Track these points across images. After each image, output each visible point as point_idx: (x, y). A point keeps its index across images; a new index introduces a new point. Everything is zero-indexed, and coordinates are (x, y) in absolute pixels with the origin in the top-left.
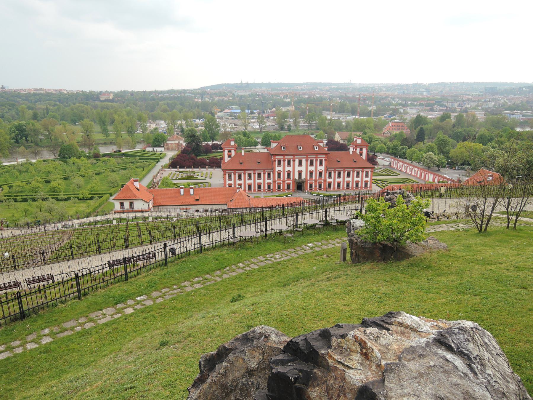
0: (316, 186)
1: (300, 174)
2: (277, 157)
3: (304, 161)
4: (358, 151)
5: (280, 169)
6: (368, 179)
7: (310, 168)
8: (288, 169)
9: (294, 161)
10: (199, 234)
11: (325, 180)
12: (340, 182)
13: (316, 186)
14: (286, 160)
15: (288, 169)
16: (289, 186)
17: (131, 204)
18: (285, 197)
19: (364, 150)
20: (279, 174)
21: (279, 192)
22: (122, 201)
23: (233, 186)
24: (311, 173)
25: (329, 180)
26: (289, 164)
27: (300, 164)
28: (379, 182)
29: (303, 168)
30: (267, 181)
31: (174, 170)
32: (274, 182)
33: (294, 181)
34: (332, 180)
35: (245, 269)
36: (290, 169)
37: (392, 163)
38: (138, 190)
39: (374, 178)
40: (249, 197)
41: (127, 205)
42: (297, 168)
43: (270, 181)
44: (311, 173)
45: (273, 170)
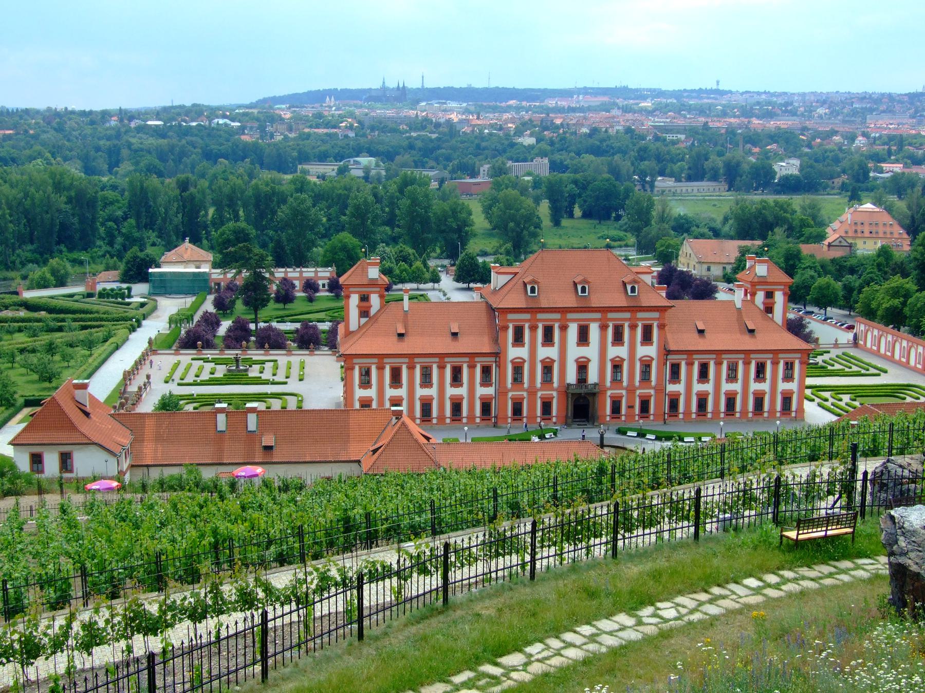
0: (631, 407)
1: (582, 367)
2: (510, 316)
3: (594, 331)
4: (760, 297)
5: (522, 352)
6: (793, 386)
7: (614, 352)
8: (544, 352)
9: (564, 328)
10: (781, 461)
11: (660, 390)
12: (707, 394)
13: (631, 407)
14: (540, 326)
15: (544, 352)
16: (547, 407)
17: (66, 461)
18: (536, 439)
20: (518, 369)
21: (517, 424)
22: (36, 450)
23: (374, 405)
24: (617, 367)
25: (671, 388)
26: (548, 338)
27: (583, 338)
28: (826, 395)
29: (591, 352)
30: (481, 391)
31: (186, 357)
32: (502, 392)
33: (566, 390)
34: (680, 388)
35: (761, 584)
36: (552, 353)
38: (87, 414)
39: (809, 381)
40: (428, 439)
41: (51, 463)
42: (574, 352)
43: (490, 391)
44: (617, 367)
45: (498, 355)
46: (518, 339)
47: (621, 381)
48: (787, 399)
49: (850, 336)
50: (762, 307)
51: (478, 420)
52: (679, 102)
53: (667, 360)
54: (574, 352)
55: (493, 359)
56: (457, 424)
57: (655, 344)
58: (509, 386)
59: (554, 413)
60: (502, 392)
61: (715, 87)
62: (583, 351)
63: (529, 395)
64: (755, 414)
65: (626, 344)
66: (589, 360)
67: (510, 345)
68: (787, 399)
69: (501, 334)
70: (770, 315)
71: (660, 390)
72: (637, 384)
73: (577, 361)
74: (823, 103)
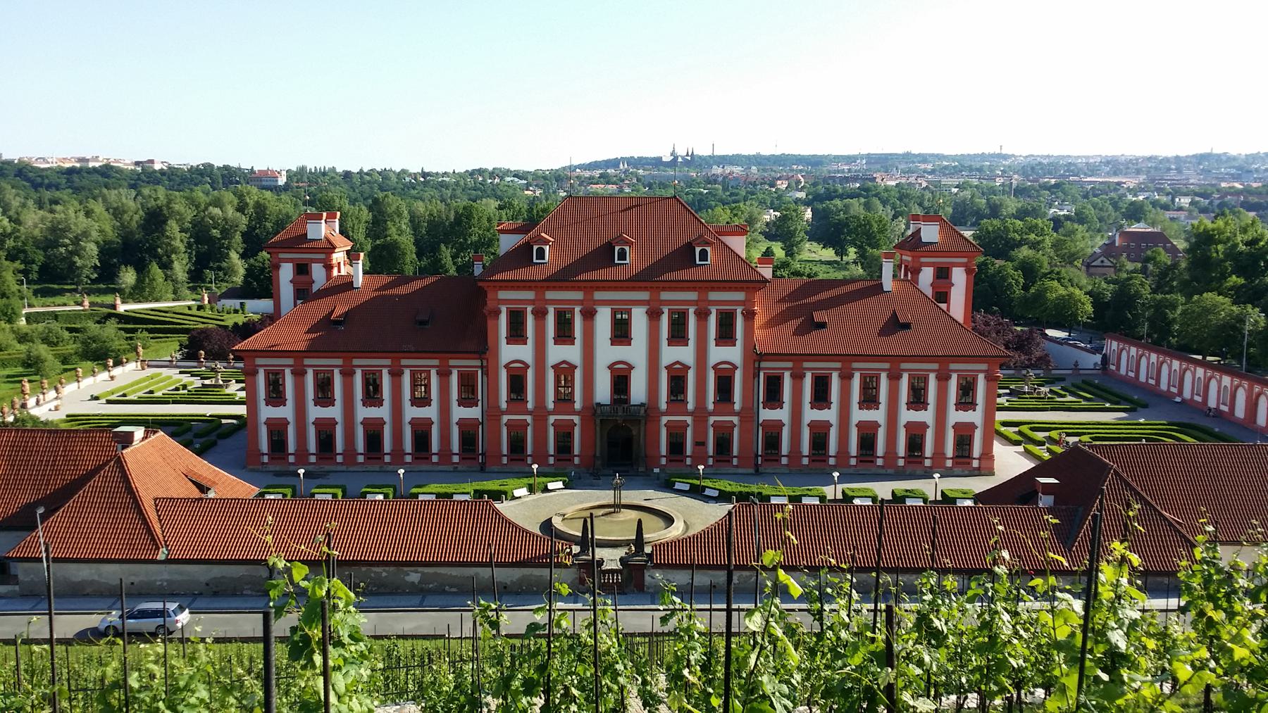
1: (621, 380)
5: (524, 352)
6: (975, 417)
7: (670, 354)
8: (556, 353)
9: (589, 315)
11: (749, 414)
14: (551, 310)
15: (556, 353)
19: (959, 277)
25: (766, 414)
26: (564, 335)
27: (621, 334)
28: (1040, 436)
30: (459, 413)
32: (492, 413)
33: (592, 411)
34: (782, 414)
36: (572, 353)
37: (1113, 359)
43: (474, 413)
46: (517, 335)
47: (685, 402)
48: (964, 436)
49: (1098, 358)
50: (929, 292)
51: (456, 459)
52: (963, 165)
53: (759, 369)
54: (607, 353)
55: (478, 363)
56: (517, 467)
57: (739, 343)
58: (504, 406)
59: (576, 451)
60: (492, 413)
61: (998, 151)
62: (621, 353)
63: (534, 420)
64: (368, 458)
65: (692, 342)
66: (631, 367)
67: (503, 341)
68: (964, 436)
69: (490, 323)
70: (943, 306)
71: (749, 414)
72: (711, 407)
73: (610, 367)
74: (1108, 163)
